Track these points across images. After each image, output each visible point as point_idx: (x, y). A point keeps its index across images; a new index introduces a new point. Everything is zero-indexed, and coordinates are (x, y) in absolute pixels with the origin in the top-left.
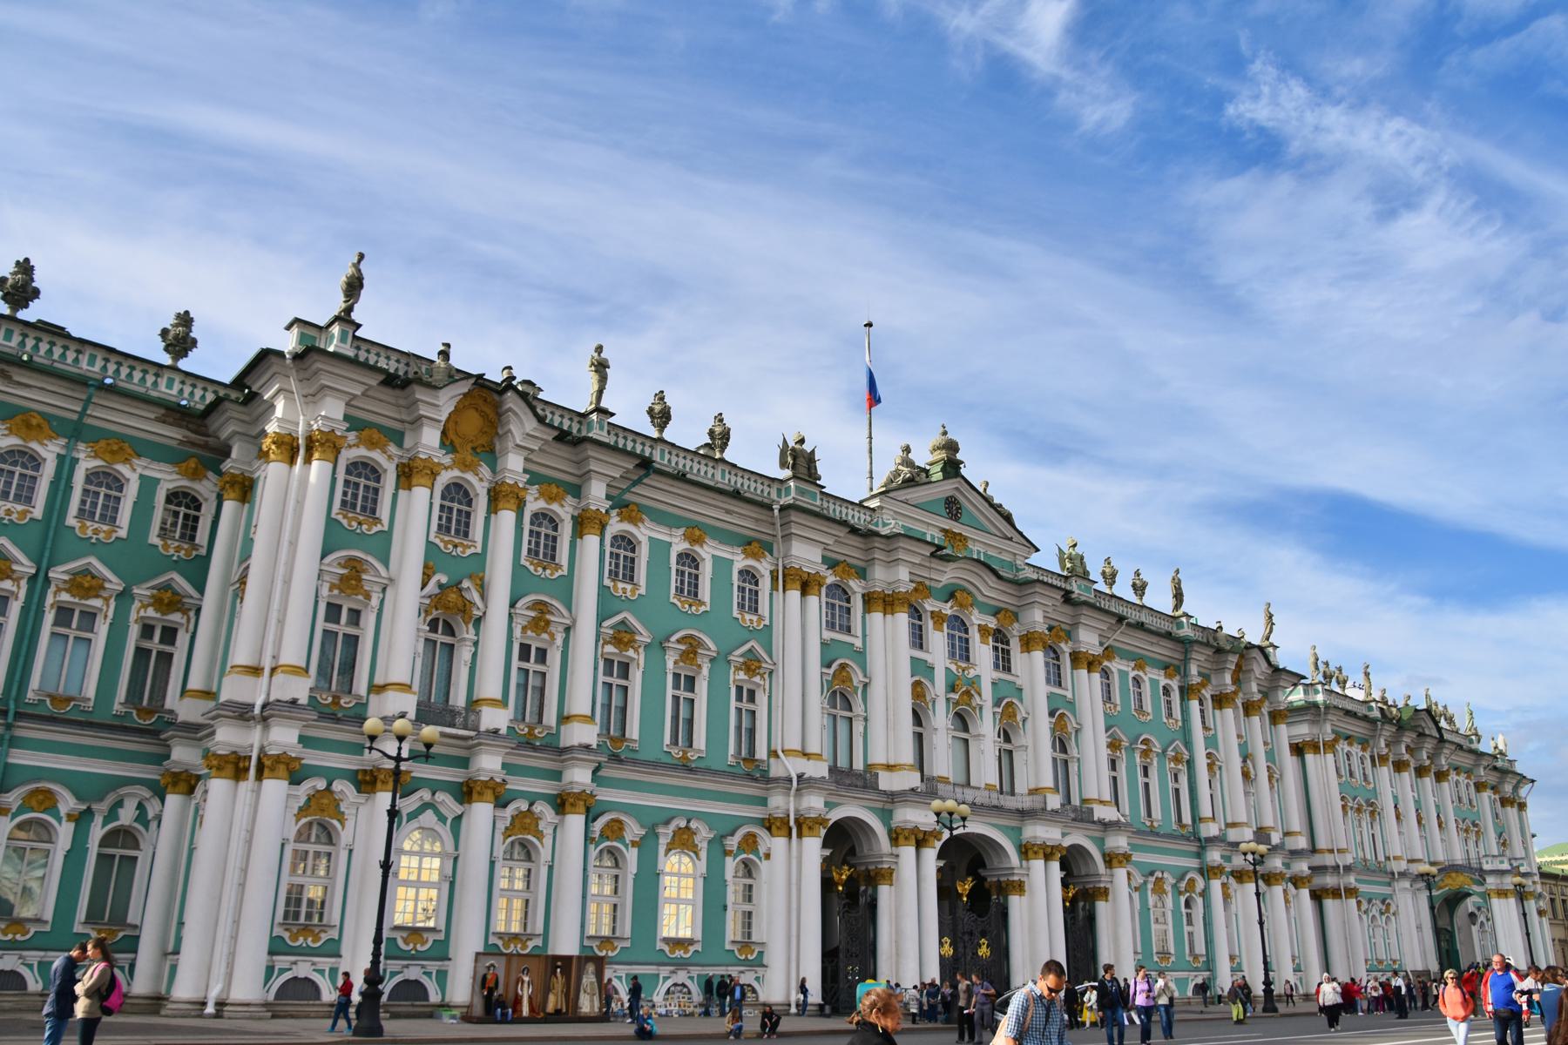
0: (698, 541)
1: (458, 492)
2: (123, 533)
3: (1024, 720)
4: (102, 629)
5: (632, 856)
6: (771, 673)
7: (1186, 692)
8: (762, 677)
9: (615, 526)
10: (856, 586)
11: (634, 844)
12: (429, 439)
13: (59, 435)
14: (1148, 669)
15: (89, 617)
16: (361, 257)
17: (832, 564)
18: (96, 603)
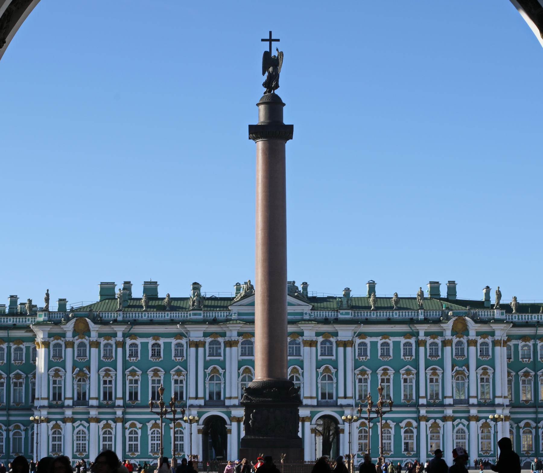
0: (159, 339)
1: (82, 345)
2: (24, 362)
3: (303, 372)
4: (24, 386)
5: (139, 432)
6: (187, 374)
7: (419, 343)
8: (184, 376)
9: (129, 342)
10: (221, 340)
11: (140, 428)
12: (69, 335)
13: (6, 342)
14: (391, 338)
15: (21, 384)
16: (48, 290)
17: (206, 335)
18: (21, 380)
